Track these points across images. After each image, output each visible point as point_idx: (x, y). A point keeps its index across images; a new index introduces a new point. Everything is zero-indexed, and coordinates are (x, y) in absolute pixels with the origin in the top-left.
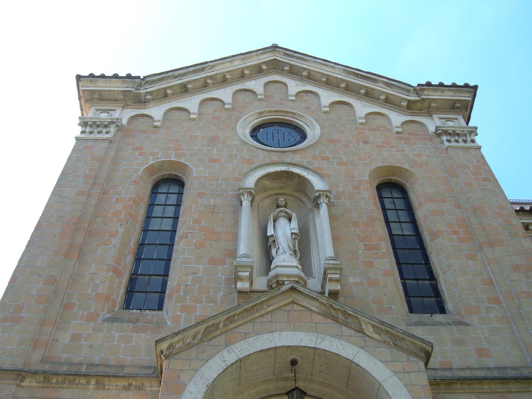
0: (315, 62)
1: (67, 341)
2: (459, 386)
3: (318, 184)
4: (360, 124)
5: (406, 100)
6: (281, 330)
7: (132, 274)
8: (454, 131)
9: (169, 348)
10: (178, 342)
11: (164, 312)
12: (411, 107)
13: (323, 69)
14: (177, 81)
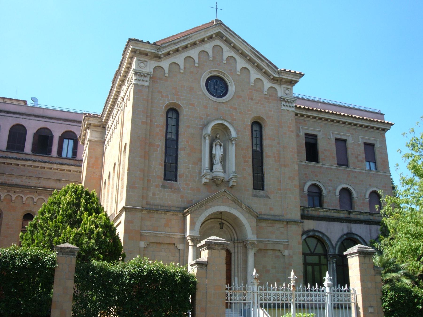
1: (151, 195)
3: (234, 134)
4: (251, 86)
5: (273, 76)
8: (287, 100)
11: (178, 183)
12: (274, 80)
13: (241, 46)
14: (175, 46)
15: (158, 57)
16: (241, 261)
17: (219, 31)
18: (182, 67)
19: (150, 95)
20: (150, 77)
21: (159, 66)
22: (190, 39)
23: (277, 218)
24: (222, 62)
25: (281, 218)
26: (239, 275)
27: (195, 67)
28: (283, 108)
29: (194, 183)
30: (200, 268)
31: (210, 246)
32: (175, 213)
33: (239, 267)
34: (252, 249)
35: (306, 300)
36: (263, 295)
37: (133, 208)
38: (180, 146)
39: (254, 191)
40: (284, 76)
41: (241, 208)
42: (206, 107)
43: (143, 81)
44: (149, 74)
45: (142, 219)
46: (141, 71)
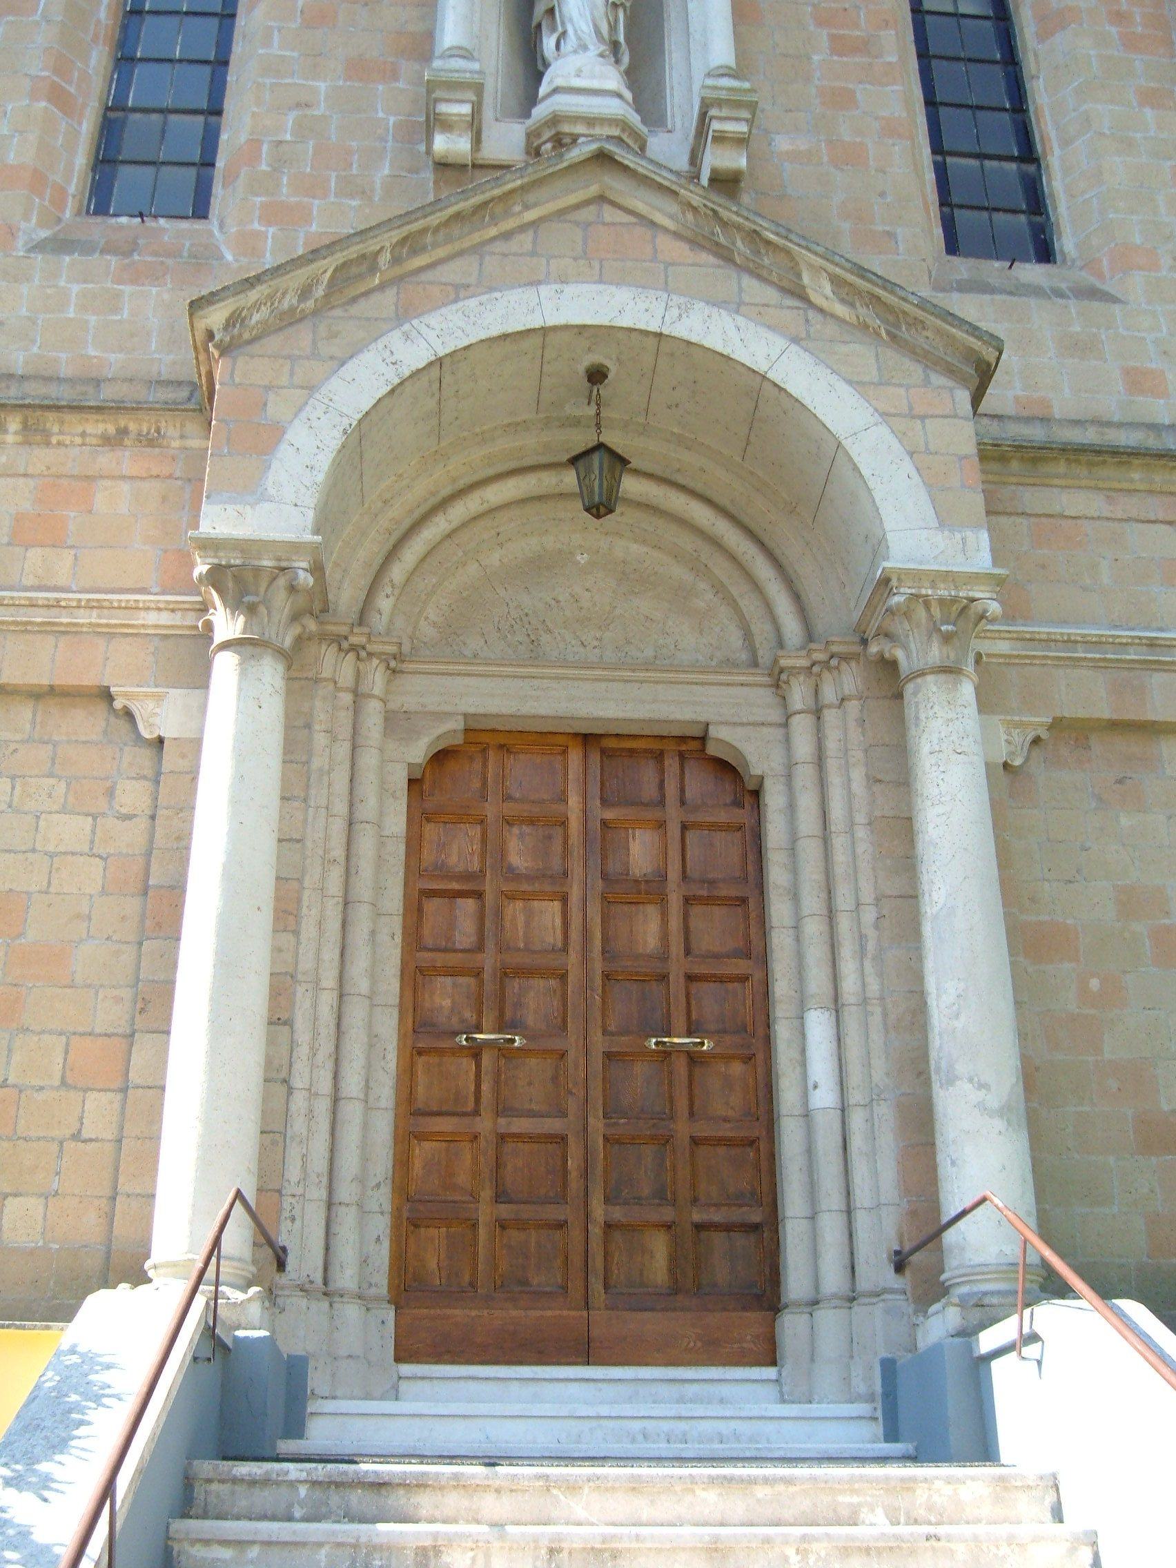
2: (1062, 467)
6: (563, 280)
7: (108, 109)
9: (229, 323)
10: (257, 306)
11: (213, 224)
16: (861, 833)
26: (849, 985)
29: (354, 203)
33: (844, 900)
34: (950, 670)
41: (790, 302)
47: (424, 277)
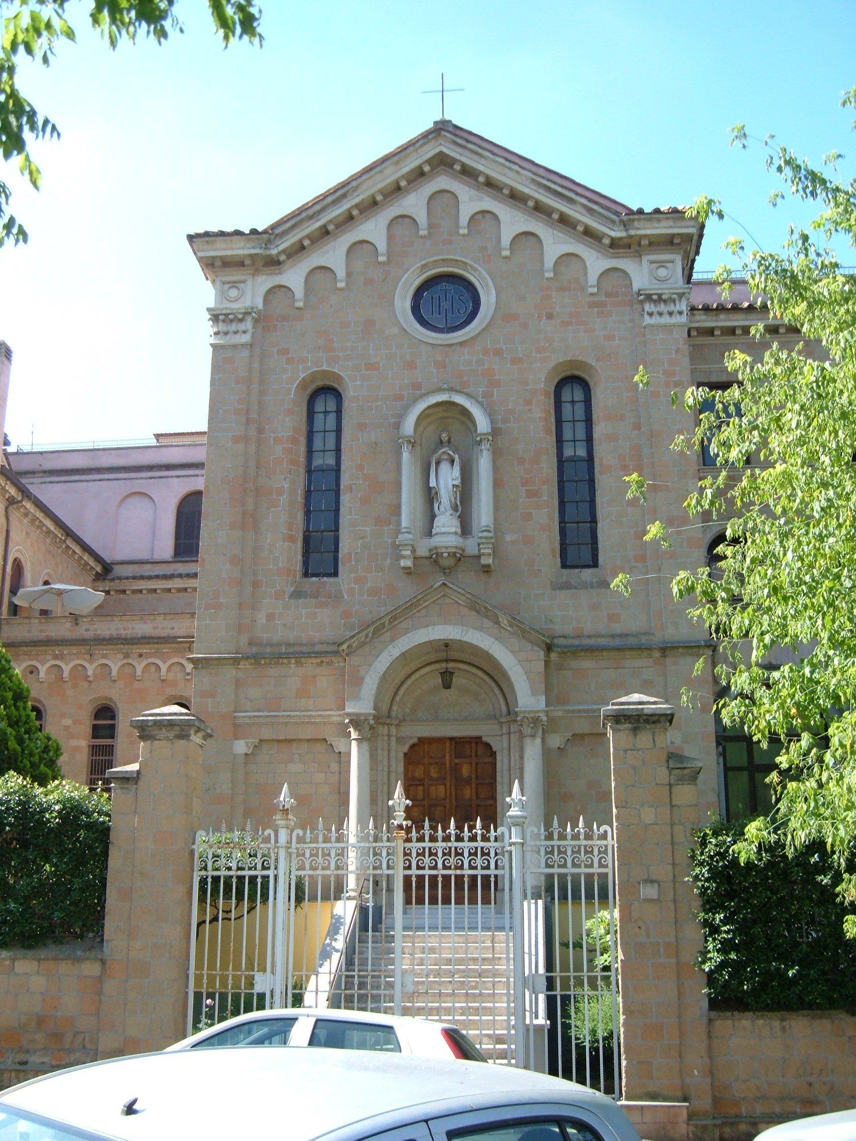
0: (495, 162)
1: (264, 621)
2: (582, 654)
4: (547, 279)
6: (435, 625)
7: (304, 532)
8: (660, 295)
9: (348, 647)
10: (354, 642)
13: (505, 175)
14: (314, 223)
15: (273, 263)
17: (437, 151)
18: (341, 273)
19: (256, 366)
20: (253, 318)
21: (280, 287)
22: (355, 194)
23: (632, 641)
24: (457, 233)
25: (644, 640)
27: (380, 263)
28: (648, 320)
29: (380, 574)
30: (122, 788)
31: (147, 733)
32: (325, 660)
35: (440, 865)
36: (308, 855)
37: (211, 659)
38: (345, 481)
39: (566, 572)
40: (644, 229)
41: (496, 626)
42: (411, 365)
43: (236, 333)
44: (250, 313)
45: (238, 684)
46: (226, 308)
47: (398, 626)
